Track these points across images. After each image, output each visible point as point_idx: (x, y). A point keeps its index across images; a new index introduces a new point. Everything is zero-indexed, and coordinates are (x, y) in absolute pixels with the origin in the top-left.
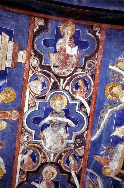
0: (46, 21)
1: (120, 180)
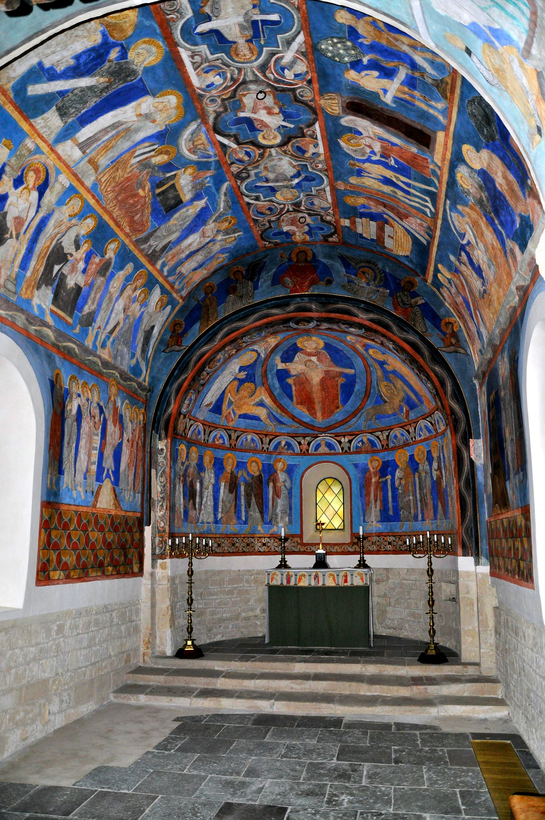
0: (326, 241)
1: (168, 175)
